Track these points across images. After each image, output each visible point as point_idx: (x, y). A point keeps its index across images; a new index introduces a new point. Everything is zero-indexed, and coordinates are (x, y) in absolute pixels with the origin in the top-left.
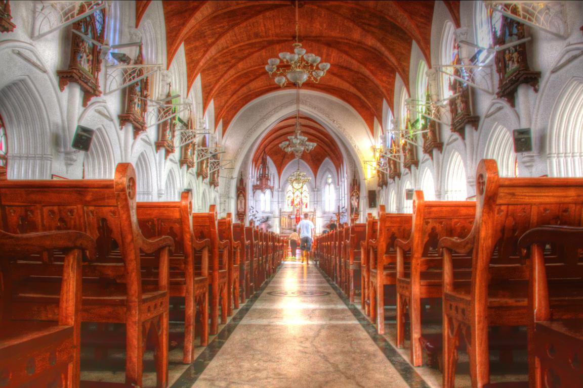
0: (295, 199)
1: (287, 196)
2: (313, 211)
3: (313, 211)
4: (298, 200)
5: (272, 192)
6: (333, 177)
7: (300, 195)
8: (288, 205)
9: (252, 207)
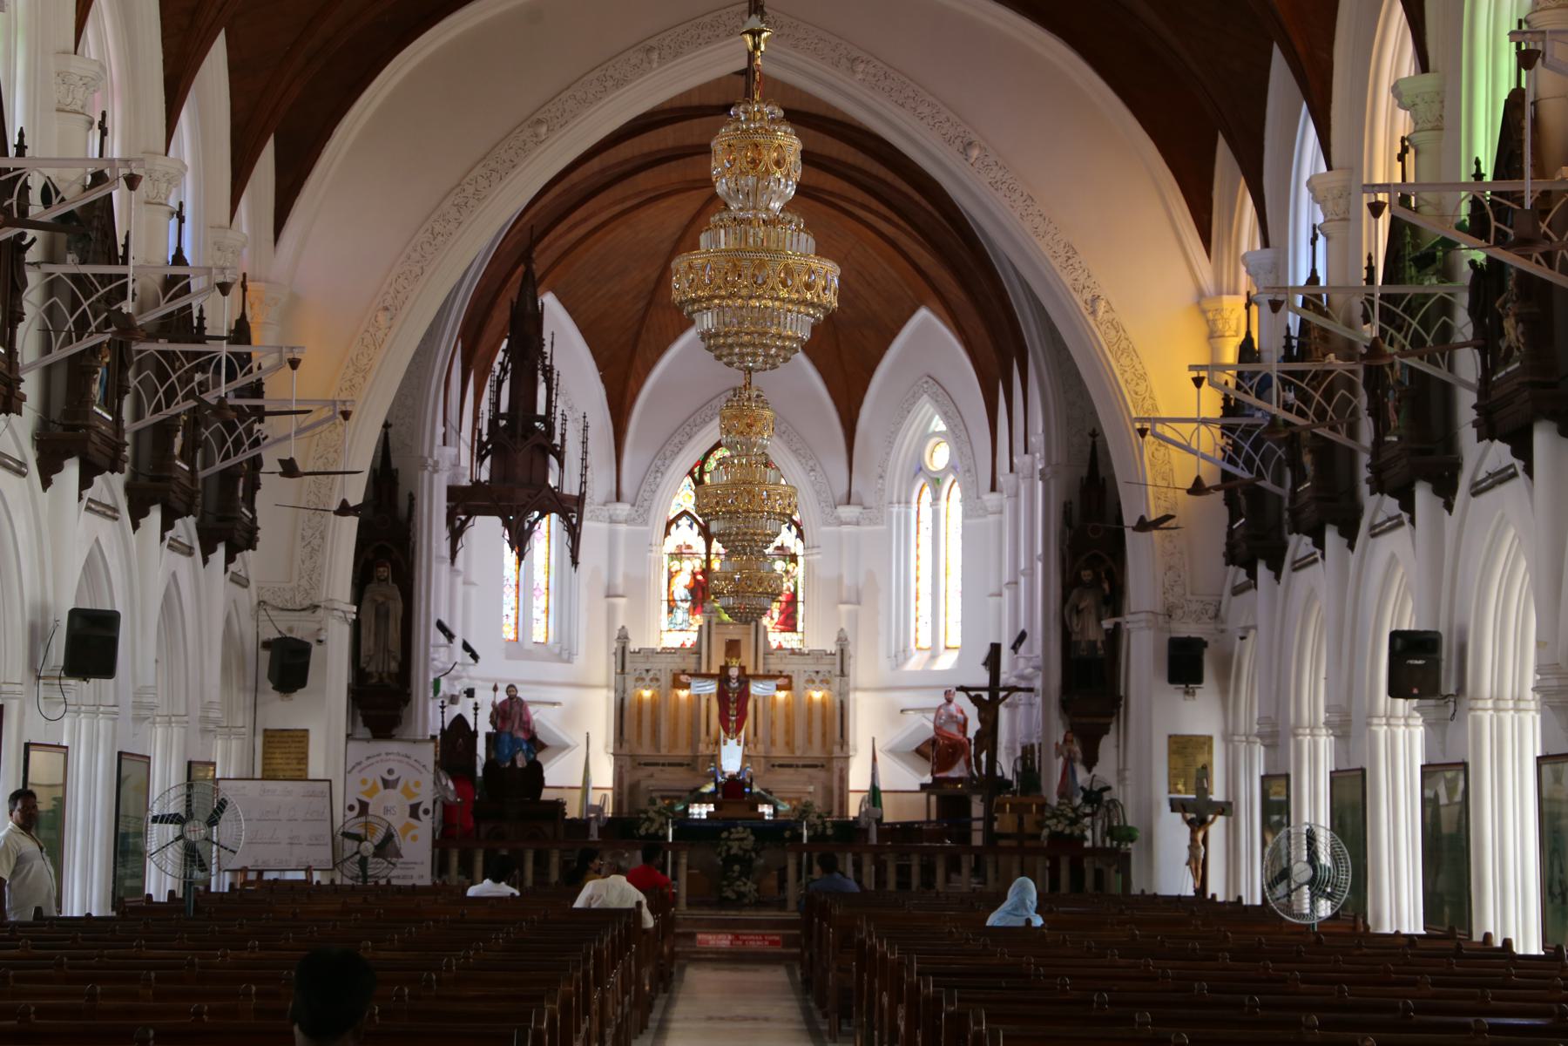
1: (671, 544)
2: (832, 647)
3: (832, 647)
5: (574, 533)
6: (958, 433)
8: (671, 611)
9: (441, 626)
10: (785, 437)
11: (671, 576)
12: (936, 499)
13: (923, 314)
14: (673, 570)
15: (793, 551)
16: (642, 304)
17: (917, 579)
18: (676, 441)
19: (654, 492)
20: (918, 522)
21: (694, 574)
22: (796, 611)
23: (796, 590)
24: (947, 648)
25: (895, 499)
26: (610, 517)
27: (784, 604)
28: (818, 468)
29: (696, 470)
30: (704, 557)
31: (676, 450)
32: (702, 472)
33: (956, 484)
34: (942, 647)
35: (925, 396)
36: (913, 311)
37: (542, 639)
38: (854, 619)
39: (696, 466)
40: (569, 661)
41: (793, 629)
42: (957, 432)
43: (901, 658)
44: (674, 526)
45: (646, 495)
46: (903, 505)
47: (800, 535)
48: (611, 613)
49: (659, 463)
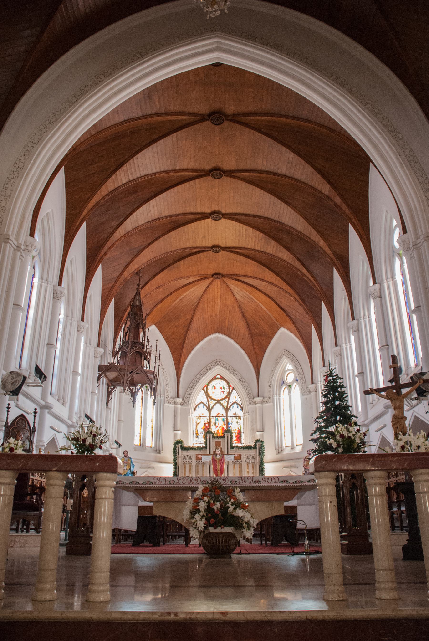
0: (213, 420)
1: (197, 414)
4: (221, 423)
7: (223, 412)
8: (197, 437)
10: (235, 375)
11: (197, 424)
12: (290, 392)
13: (282, 330)
14: (198, 422)
15: (239, 415)
16: (186, 329)
18: (198, 377)
19: (190, 395)
21: (205, 424)
22: (241, 436)
23: (241, 429)
25: (275, 394)
26: (175, 403)
27: (237, 434)
28: (247, 385)
29: (205, 388)
30: (208, 418)
31: (198, 380)
32: (207, 389)
33: (297, 386)
34: (295, 445)
35: (284, 356)
36: (278, 329)
37: (150, 446)
38: (263, 436)
39: (205, 387)
40: (159, 453)
41: (240, 442)
42: (297, 366)
43: (280, 450)
44: (198, 407)
45: (188, 396)
46: (278, 396)
47: (242, 409)
48: (175, 435)
49: (192, 385)
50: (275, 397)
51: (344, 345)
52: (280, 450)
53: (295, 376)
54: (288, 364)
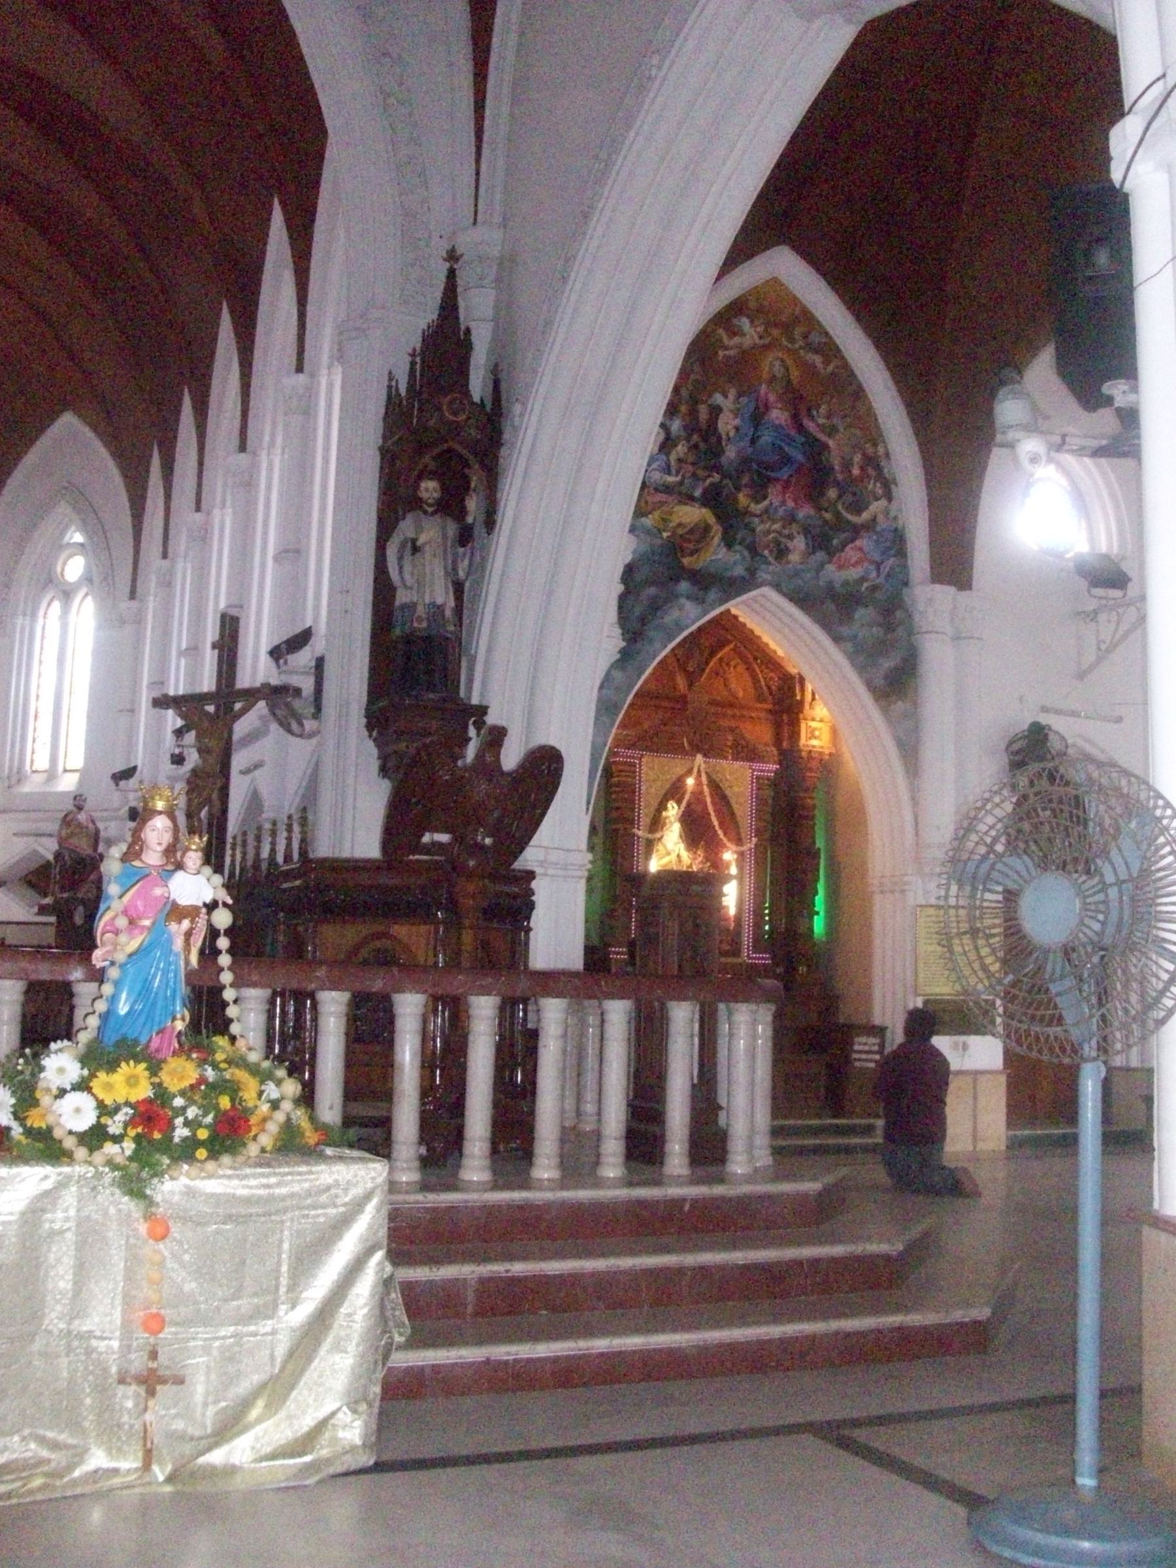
13: (68, 421)
17: (38, 696)
20: (43, 637)
24: (65, 771)
33: (89, 598)
34: (60, 769)
46: (28, 618)
50: (19, 621)
51: (216, 512)
52: (14, 780)
53: (88, 568)
54: (73, 528)
